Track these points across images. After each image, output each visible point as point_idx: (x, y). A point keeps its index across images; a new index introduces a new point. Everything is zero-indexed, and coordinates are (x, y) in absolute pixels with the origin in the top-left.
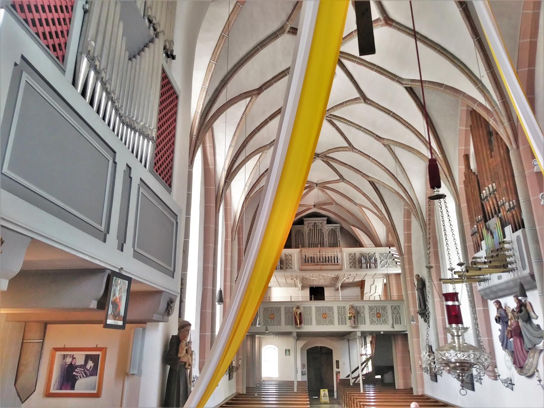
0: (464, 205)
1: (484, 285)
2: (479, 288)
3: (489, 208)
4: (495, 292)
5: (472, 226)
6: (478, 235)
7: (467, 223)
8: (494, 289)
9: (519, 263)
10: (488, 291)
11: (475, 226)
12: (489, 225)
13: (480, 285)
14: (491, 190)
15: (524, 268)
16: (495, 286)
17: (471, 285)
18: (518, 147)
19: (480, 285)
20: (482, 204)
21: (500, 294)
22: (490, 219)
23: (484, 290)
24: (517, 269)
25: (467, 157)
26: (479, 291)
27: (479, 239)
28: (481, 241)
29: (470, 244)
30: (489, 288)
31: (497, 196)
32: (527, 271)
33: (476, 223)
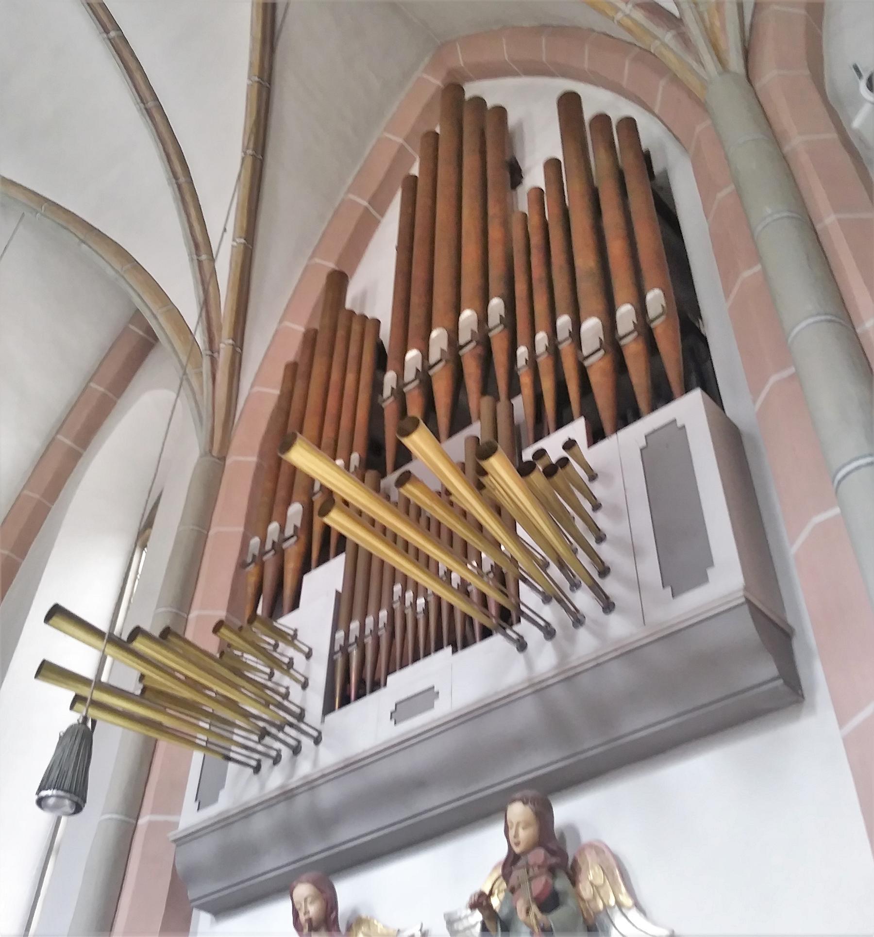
4: (323, 822)
5: (255, 523)
8: (328, 796)
16: (351, 767)
28: (306, 567)
30: (287, 795)
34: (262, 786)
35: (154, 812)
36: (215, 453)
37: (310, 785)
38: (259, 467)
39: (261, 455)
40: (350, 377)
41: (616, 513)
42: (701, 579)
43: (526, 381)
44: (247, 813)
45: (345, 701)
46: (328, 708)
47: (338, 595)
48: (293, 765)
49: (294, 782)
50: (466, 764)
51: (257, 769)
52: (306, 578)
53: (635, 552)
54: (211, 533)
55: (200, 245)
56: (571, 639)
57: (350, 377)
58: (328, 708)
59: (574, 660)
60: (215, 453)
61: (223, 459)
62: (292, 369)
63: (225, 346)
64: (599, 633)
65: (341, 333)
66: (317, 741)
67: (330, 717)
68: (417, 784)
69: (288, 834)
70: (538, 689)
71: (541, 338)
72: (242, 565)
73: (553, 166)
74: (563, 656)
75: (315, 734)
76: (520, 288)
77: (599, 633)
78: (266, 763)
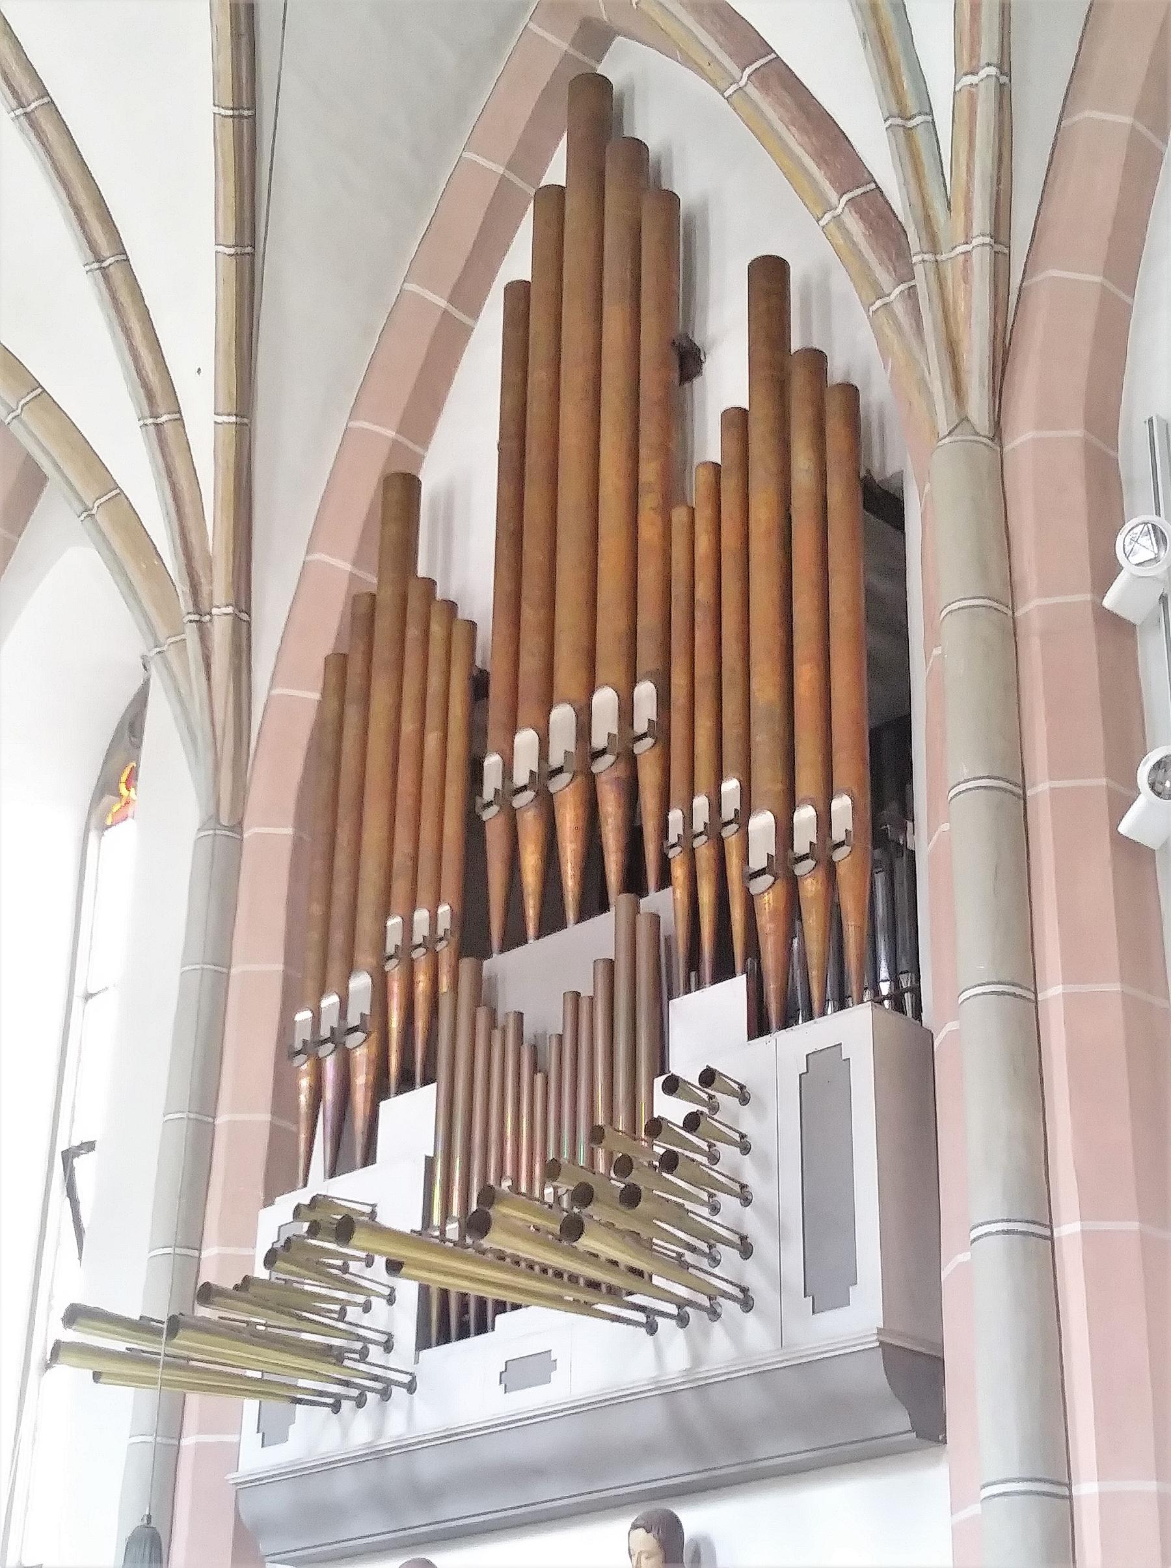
0: (272, 831)
1: (314, 1434)
2: (256, 1458)
3: (531, 860)
4: (426, 1495)
6: (362, 1055)
7: (260, 964)
8: (429, 1467)
9: (781, 1258)
10: (345, 1485)
11: (361, 983)
12: (493, 981)
13: (269, 1435)
14: (604, 726)
15: (826, 1286)
16: (451, 1439)
17: (171, 1425)
18: (997, 431)
19: (269, 1435)
20: (474, 828)
21: (457, 1510)
22: (514, 938)
23: (299, 1475)
24: (747, 1303)
25: (402, 492)
26: (257, 1483)
27: (361, 1080)
28: (380, 1091)
29: (245, 1114)
30: (378, 1456)
31: (649, 777)
32: (862, 1316)
33: (365, 957)
34: (345, 1434)
35: (200, 1432)
36: (224, 821)
37: (407, 1450)
38: (298, 844)
39: (300, 822)
40: (432, 739)
41: (766, 1166)
42: (843, 1301)
43: (679, 872)
44: (329, 1467)
45: (444, 1338)
46: (423, 1342)
47: (430, 1163)
48: (383, 1414)
49: (384, 1443)
50: (585, 1461)
51: (336, 1408)
52: (383, 1105)
53: (781, 1235)
54: (233, 971)
55: (157, 396)
56: (706, 1334)
57: (432, 739)
58: (423, 1342)
59: (704, 1370)
60: (224, 821)
61: (237, 826)
62: (338, 664)
63: (219, 587)
64: (736, 1335)
65: (413, 632)
66: (411, 1388)
67: (424, 1353)
68: (532, 1472)
69: (381, 1499)
70: (668, 1395)
71: (701, 803)
72: (286, 1052)
73: (737, 422)
74: (696, 1359)
75: (406, 1379)
76: (679, 680)
77: (736, 1335)
78: (346, 1405)
